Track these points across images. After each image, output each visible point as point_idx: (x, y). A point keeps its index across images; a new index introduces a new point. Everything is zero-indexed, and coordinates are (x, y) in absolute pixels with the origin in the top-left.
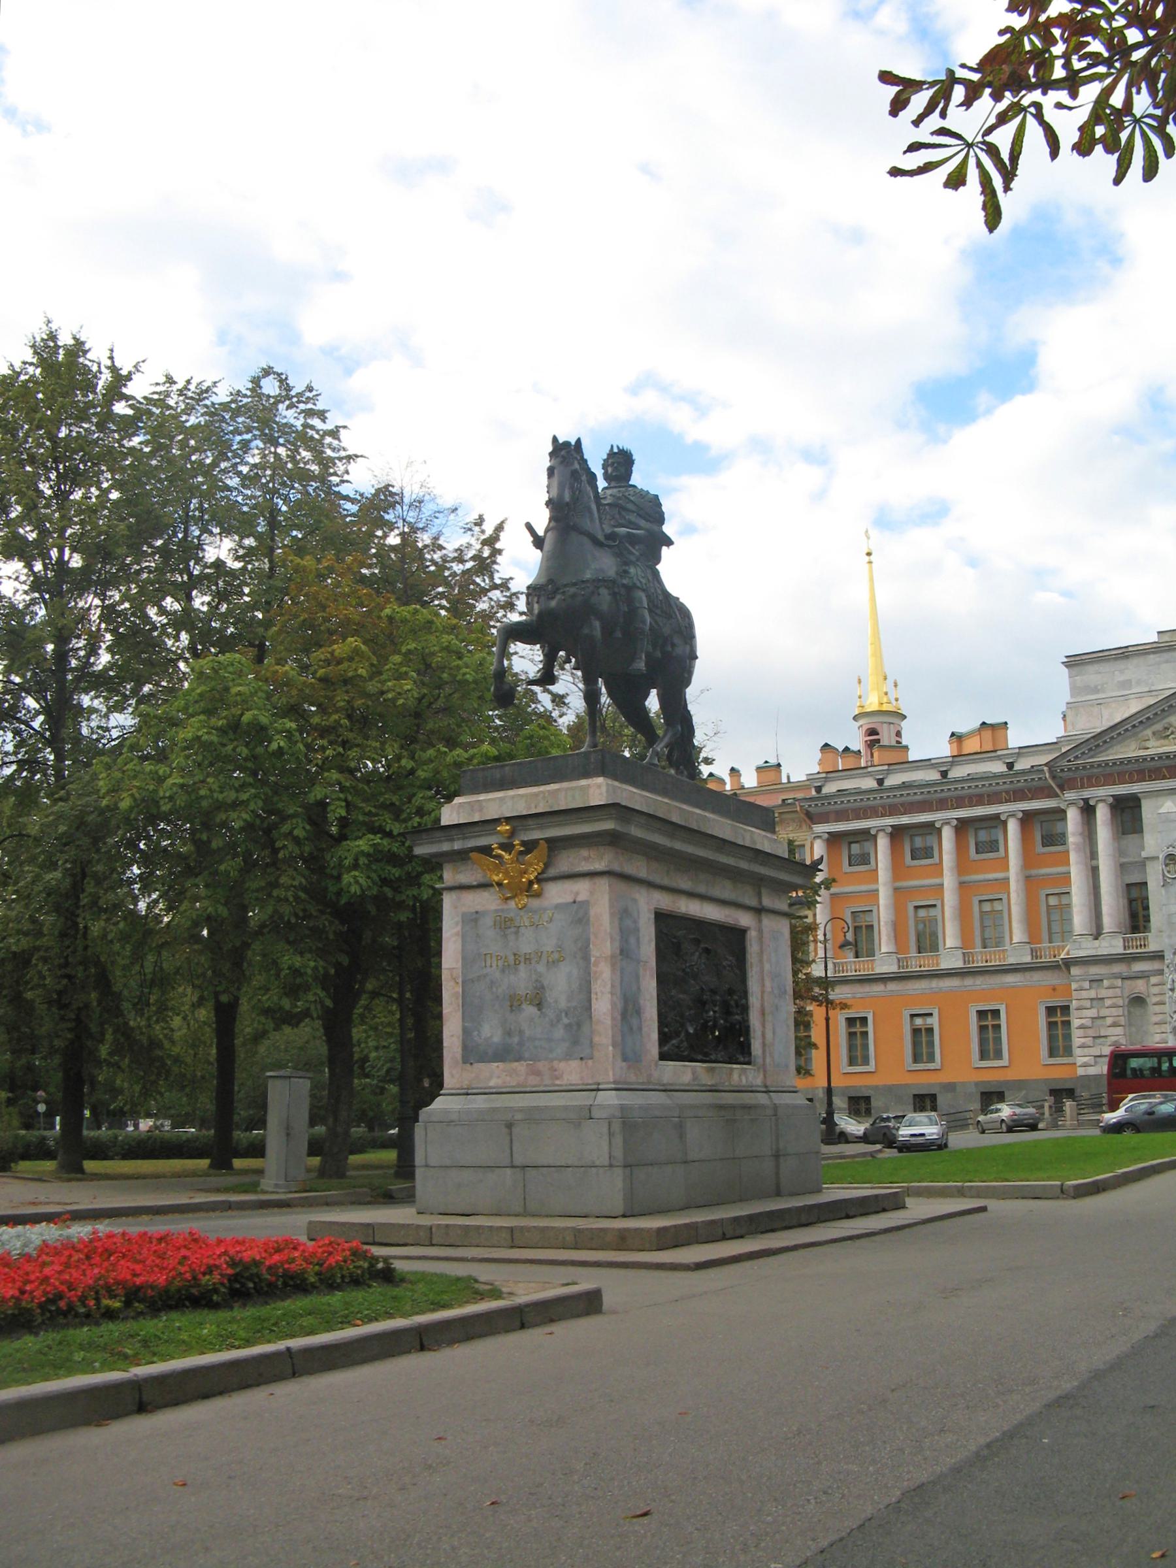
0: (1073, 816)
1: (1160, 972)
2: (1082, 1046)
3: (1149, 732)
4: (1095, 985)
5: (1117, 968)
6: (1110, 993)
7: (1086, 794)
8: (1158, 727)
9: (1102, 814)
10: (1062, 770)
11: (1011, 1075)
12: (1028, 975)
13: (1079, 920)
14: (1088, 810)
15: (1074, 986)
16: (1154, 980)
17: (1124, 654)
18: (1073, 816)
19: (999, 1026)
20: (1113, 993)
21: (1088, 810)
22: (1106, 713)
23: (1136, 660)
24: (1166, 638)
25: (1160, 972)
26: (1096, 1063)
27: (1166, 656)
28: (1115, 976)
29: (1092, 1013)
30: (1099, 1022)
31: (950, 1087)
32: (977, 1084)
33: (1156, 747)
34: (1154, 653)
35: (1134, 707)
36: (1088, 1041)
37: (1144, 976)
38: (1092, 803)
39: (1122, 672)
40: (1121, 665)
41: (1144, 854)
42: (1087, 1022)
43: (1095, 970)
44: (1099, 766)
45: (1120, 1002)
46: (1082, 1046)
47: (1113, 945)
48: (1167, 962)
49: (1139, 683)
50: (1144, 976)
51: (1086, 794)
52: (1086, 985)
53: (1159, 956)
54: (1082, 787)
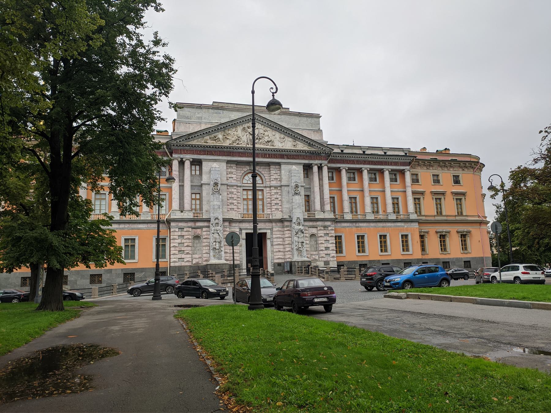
0: (175, 164)
1: (209, 227)
2: (174, 254)
3: (208, 137)
4: (180, 230)
5: (190, 224)
6: (187, 233)
7: (182, 156)
8: (213, 136)
9: (187, 164)
10: (174, 145)
11: (139, 266)
12: (149, 225)
13: (176, 205)
14: (182, 163)
15: (172, 230)
16: (204, 229)
17: (200, 107)
18: (175, 164)
19: (133, 246)
20: (188, 234)
21: (182, 163)
22: (191, 127)
23: (204, 110)
25: (209, 227)
27: (216, 111)
28: (189, 227)
29: (179, 241)
30: (182, 245)
31: (142, 270)
32: (122, 270)
33: (211, 143)
35: (203, 127)
36: (177, 252)
37: (201, 228)
38: (184, 160)
39: (198, 113)
40: (199, 111)
41: (202, 182)
42: (177, 245)
43: (181, 224)
44: (189, 146)
45: (191, 238)
46: (174, 254)
47: (190, 215)
48: (211, 222)
49: (205, 119)
50: (201, 228)
51: (182, 156)
52: (177, 230)
53: (208, 220)
54: (181, 153)
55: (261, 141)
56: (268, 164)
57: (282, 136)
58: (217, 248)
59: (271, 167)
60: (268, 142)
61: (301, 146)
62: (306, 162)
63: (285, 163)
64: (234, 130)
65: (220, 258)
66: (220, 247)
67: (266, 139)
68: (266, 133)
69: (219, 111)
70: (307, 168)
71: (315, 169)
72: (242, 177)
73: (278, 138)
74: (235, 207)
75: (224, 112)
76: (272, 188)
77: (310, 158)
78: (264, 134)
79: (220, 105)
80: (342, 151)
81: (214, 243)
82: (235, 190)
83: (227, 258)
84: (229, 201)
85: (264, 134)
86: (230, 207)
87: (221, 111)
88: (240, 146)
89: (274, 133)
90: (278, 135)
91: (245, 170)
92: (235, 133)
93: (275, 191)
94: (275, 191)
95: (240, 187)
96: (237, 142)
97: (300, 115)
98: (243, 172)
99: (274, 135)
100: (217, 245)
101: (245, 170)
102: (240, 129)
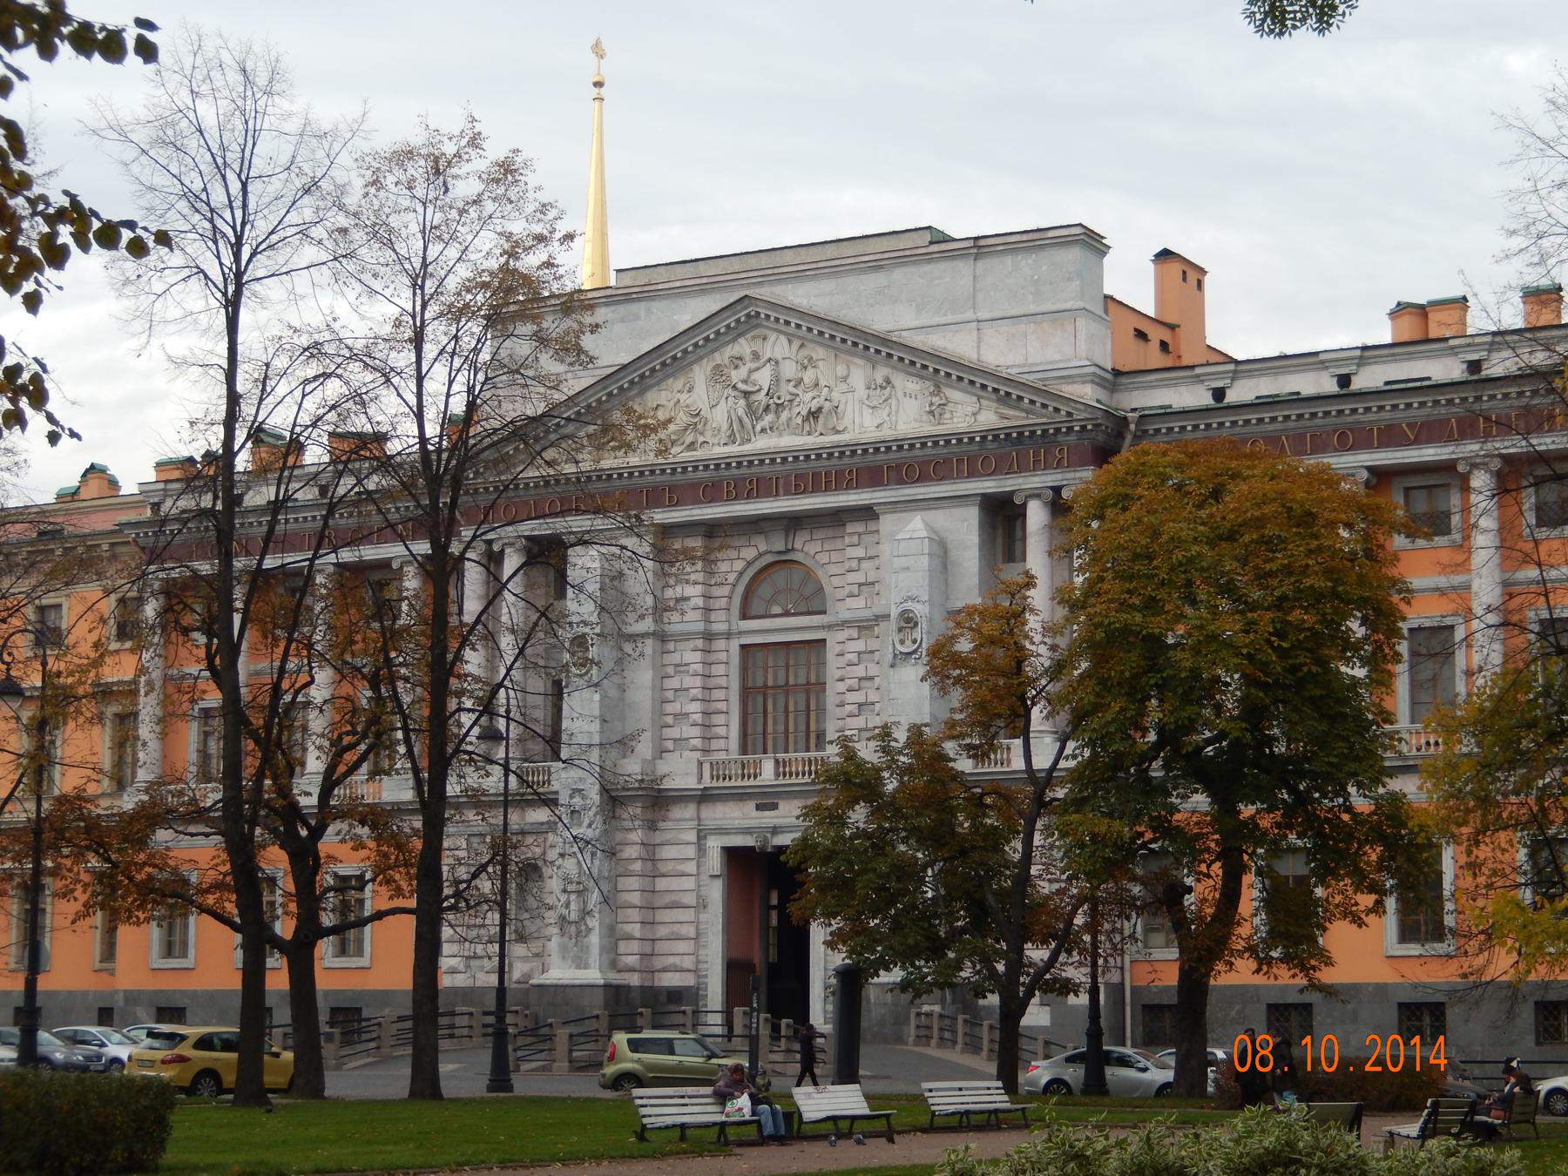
14: (493, 560)
21: (493, 560)
24: (627, 280)
26: (468, 967)
34: (607, 304)
55: (785, 415)
56: (837, 519)
57: (881, 373)
58: (573, 916)
59: (850, 528)
60: (814, 415)
61: (970, 415)
62: (990, 485)
63: (895, 506)
64: (679, 384)
65: (581, 963)
66: (585, 913)
67: (808, 401)
68: (808, 376)
69: (634, 307)
70: (1002, 518)
71: (1036, 516)
72: (740, 589)
73: (861, 392)
74: (696, 731)
75: (655, 306)
76: (847, 633)
77: (1002, 467)
78: (799, 382)
79: (642, 278)
80: (1219, 394)
81: (563, 898)
82: (697, 656)
83: (631, 960)
84: (669, 708)
85: (799, 382)
86: (674, 733)
87: (640, 308)
88: (698, 454)
89: (841, 370)
90: (860, 373)
91: (749, 554)
92: (683, 397)
93: (859, 645)
94: (859, 645)
95: (728, 635)
96: (689, 439)
97: (979, 247)
98: (739, 565)
99: (845, 379)
100: (573, 906)
101: (749, 554)
102: (700, 374)
